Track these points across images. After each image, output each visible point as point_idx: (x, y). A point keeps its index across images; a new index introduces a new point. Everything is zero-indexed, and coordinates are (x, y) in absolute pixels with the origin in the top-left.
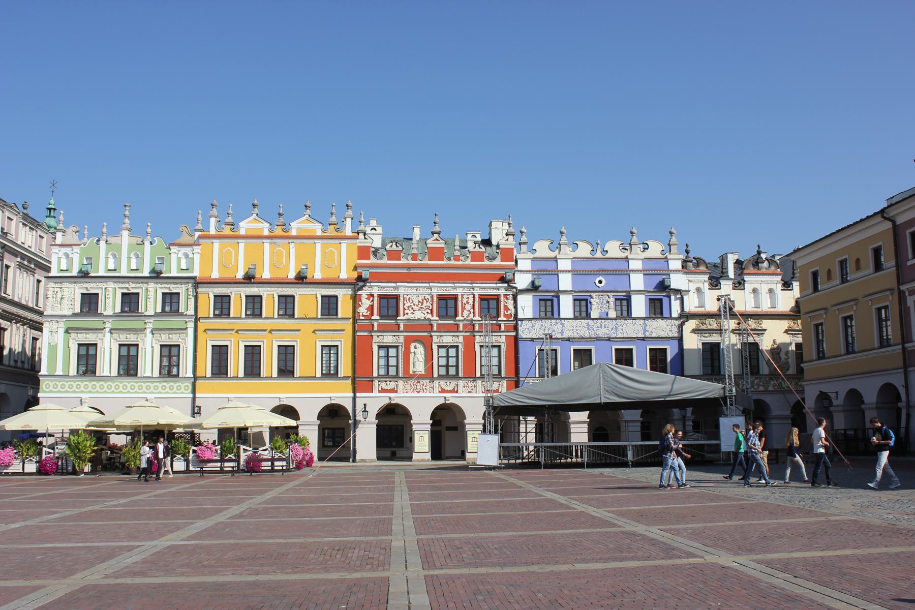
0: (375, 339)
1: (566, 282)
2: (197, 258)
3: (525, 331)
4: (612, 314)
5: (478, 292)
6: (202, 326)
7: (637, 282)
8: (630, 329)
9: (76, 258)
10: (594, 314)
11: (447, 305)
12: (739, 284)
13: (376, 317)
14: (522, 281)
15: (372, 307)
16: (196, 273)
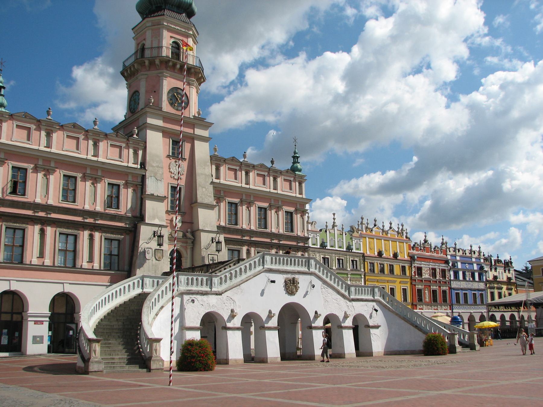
0: (417, 286)
1: (459, 265)
2: (361, 243)
3: (454, 285)
4: (471, 279)
5: (441, 268)
6: (367, 277)
7: (475, 267)
8: (475, 285)
9: (318, 238)
10: (467, 279)
11: (434, 272)
12: (496, 269)
13: (417, 276)
14: (450, 264)
15: (415, 272)
16: (362, 252)
